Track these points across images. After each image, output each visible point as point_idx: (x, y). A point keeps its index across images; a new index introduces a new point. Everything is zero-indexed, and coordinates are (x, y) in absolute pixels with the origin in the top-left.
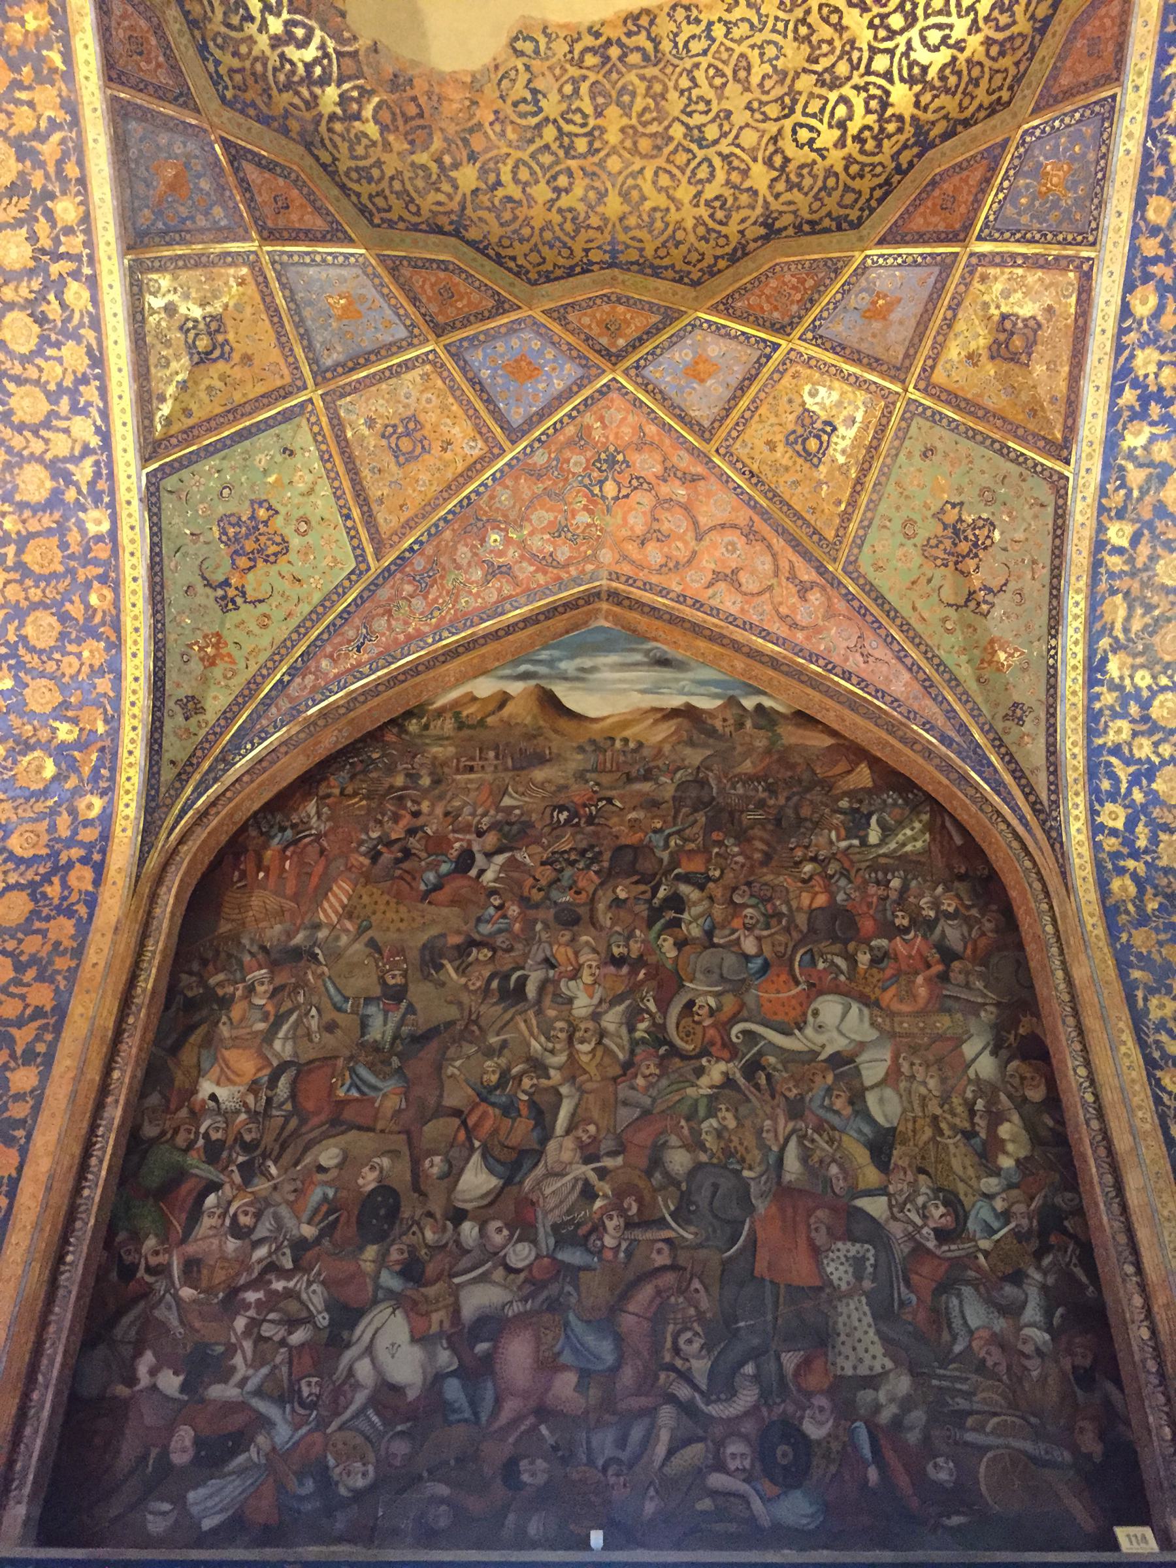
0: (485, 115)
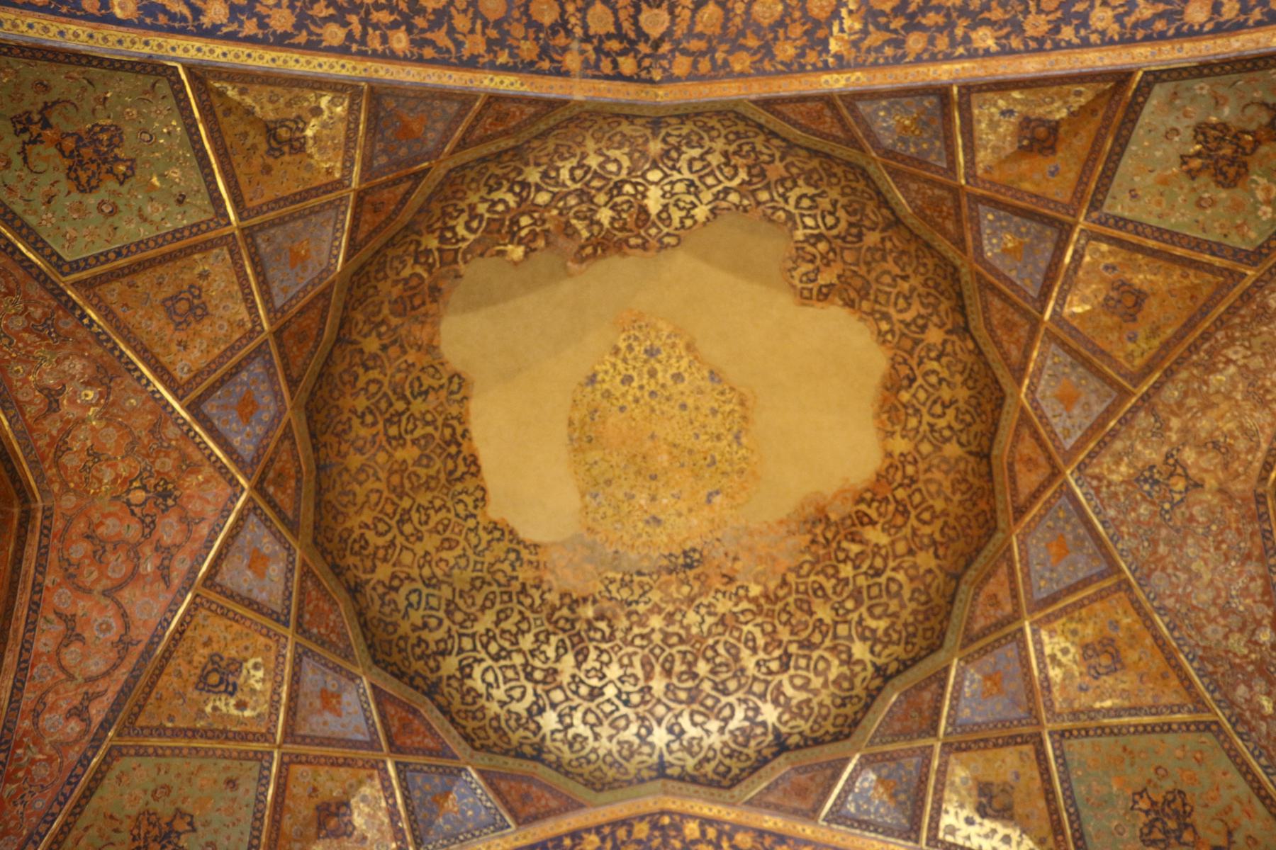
0: (411, 357)
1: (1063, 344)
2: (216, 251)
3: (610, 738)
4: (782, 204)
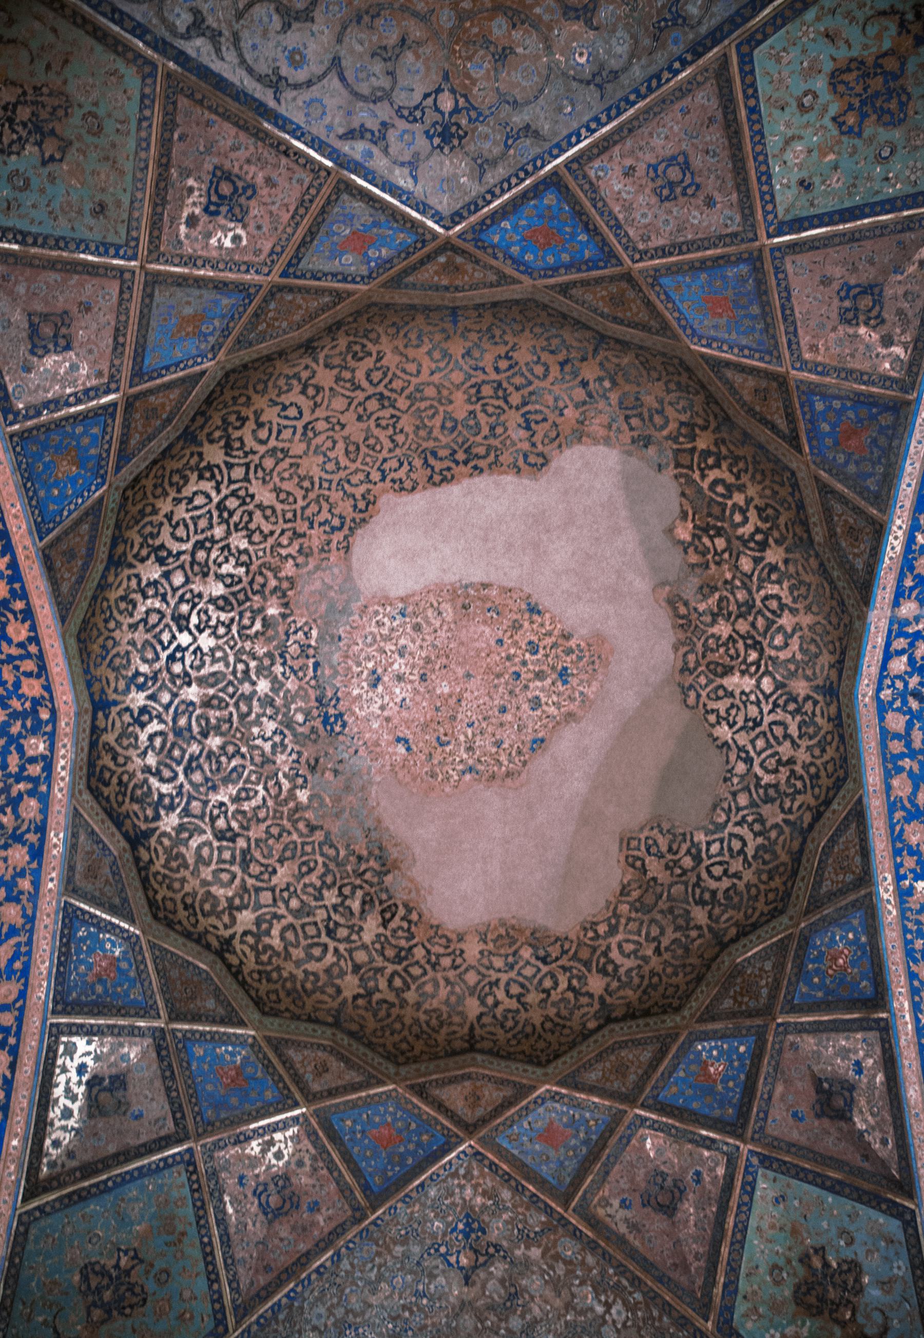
1: (610, 1130)
2: (738, 218)
3: (132, 643)
4: (734, 819)
